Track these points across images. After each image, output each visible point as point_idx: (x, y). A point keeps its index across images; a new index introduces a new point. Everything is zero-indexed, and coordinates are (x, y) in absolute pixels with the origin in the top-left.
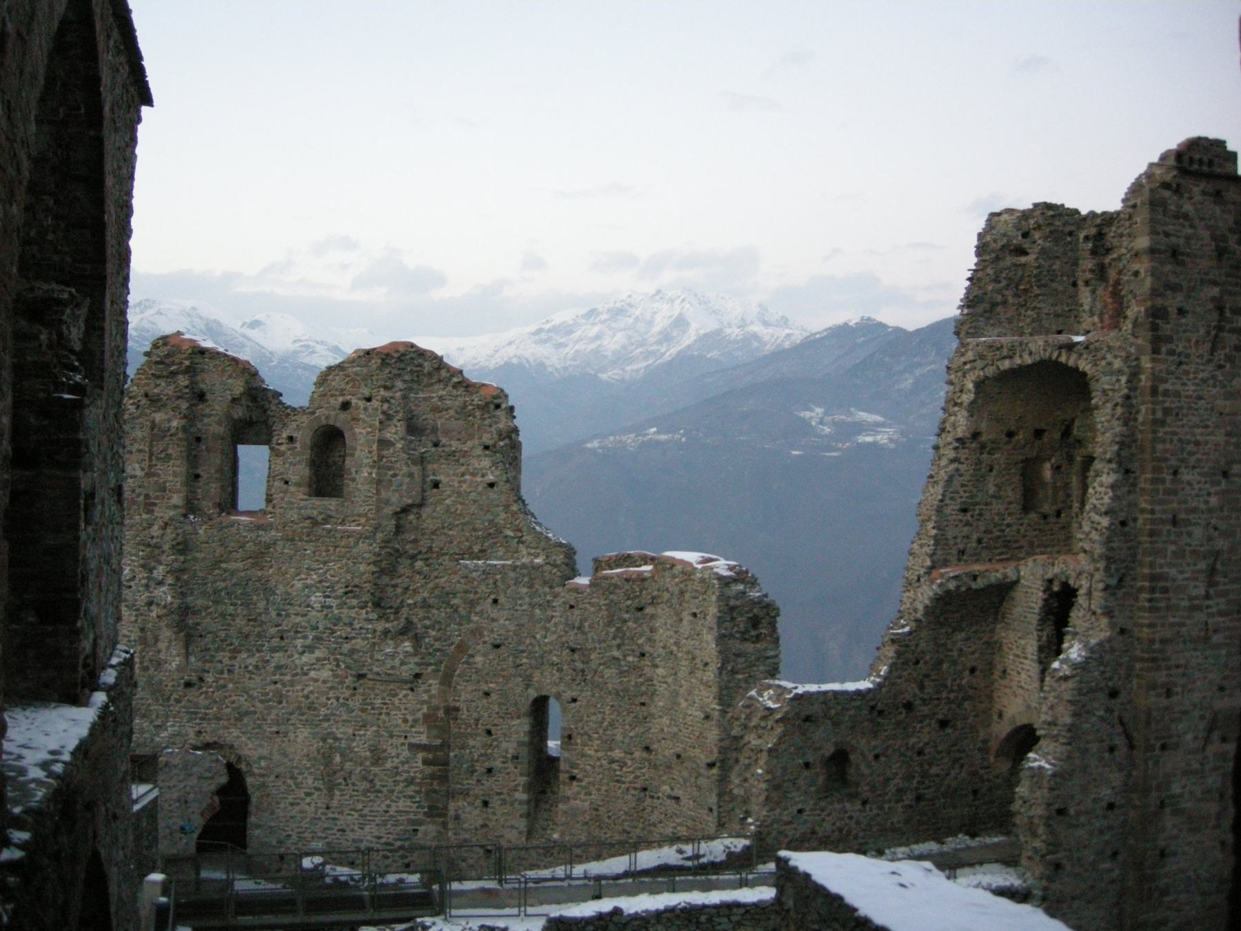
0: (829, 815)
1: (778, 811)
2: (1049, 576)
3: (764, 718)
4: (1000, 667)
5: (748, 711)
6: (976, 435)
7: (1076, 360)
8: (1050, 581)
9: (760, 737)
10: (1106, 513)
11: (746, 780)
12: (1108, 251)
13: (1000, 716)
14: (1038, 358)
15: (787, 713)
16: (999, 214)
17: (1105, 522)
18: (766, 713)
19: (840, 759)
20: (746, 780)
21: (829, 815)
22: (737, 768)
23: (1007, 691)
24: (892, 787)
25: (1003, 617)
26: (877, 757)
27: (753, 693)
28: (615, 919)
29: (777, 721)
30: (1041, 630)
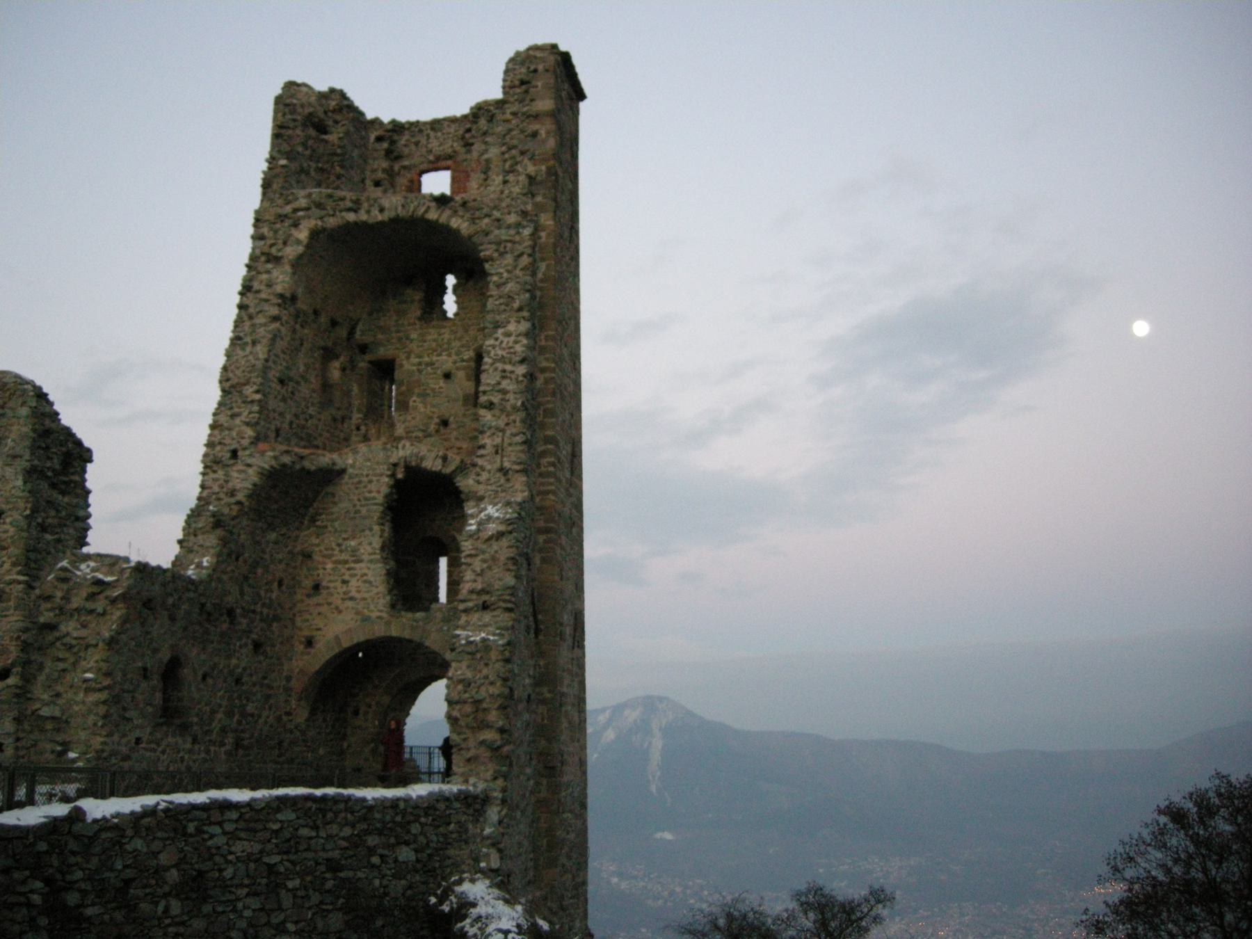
0: (163, 752)
1: (116, 738)
2: (393, 460)
3: (92, 597)
4: (308, 583)
5: (65, 587)
6: (294, 298)
7: (450, 217)
8: (395, 465)
9: (84, 626)
10: (522, 361)
11: (58, 695)
12: (399, 158)
13: (309, 643)
14: (393, 214)
15: (129, 588)
16: (298, 85)
17: (521, 370)
18: (95, 589)
19: (171, 672)
20: (58, 695)
21: (163, 752)
22: (42, 678)
23: (324, 609)
24: (216, 726)
25: (313, 520)
26: (204, 677)
27: (65, 563)
28: (77, 828)
29: (113, 601)
30: (383, 524)
